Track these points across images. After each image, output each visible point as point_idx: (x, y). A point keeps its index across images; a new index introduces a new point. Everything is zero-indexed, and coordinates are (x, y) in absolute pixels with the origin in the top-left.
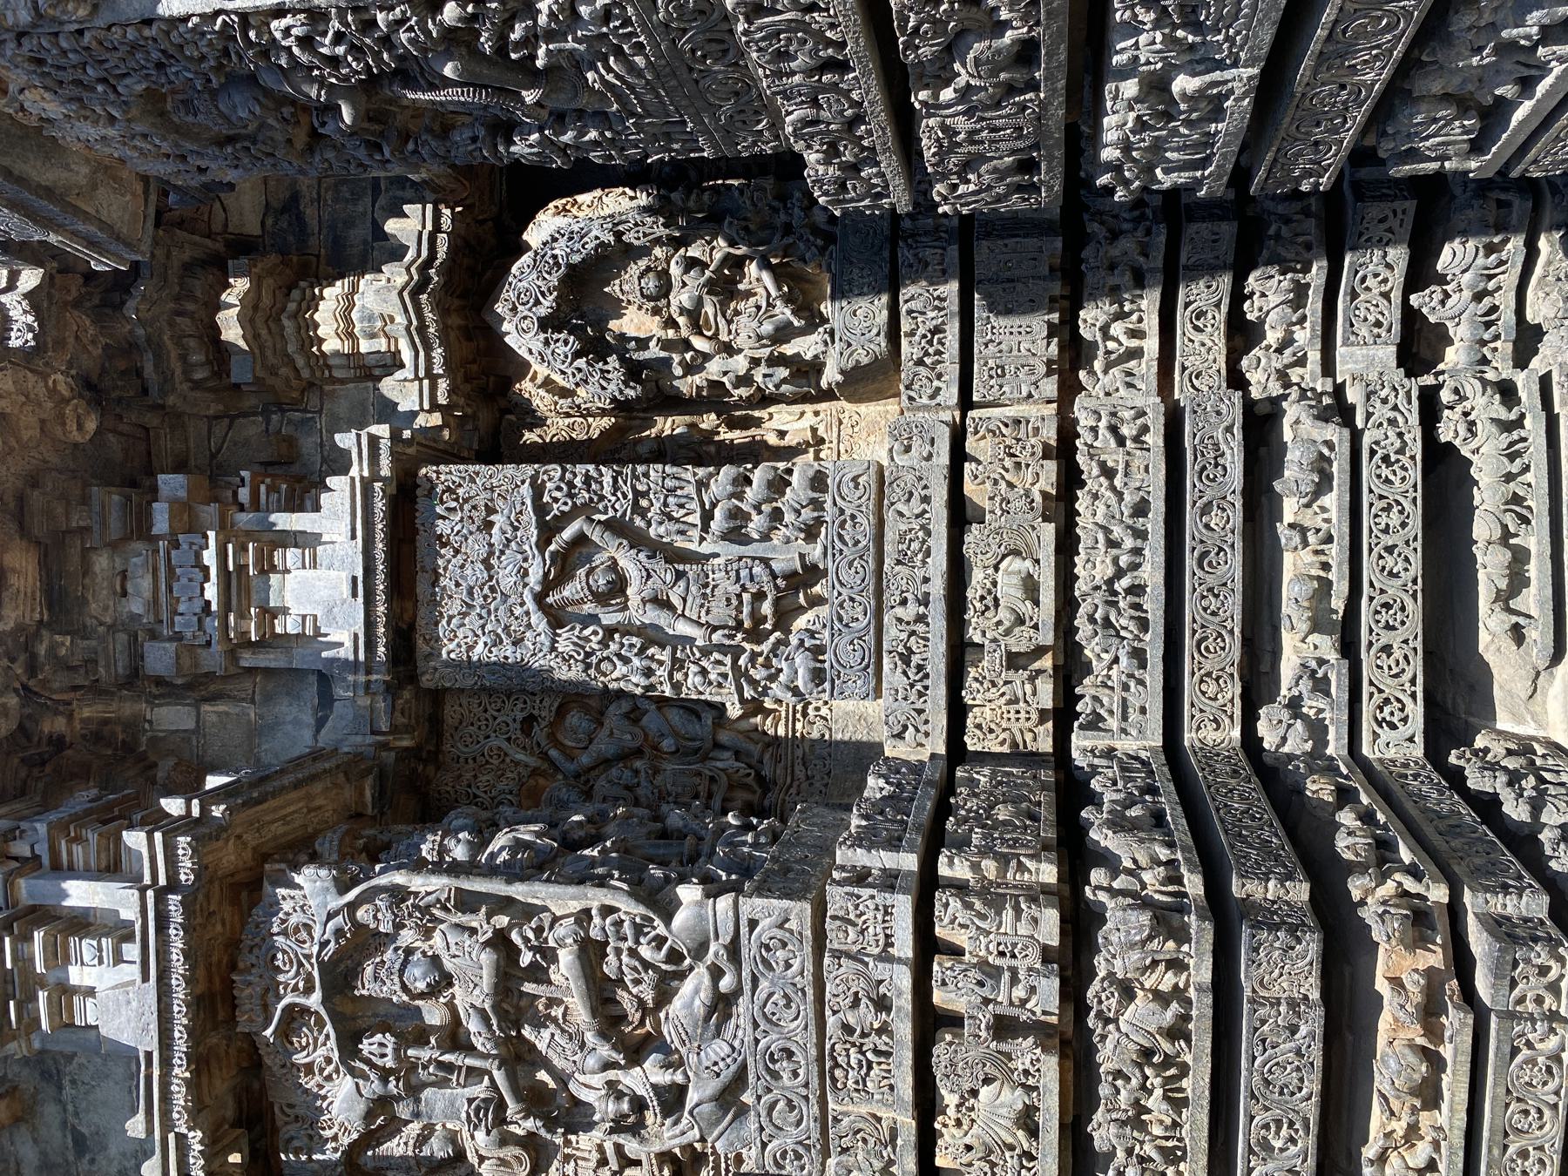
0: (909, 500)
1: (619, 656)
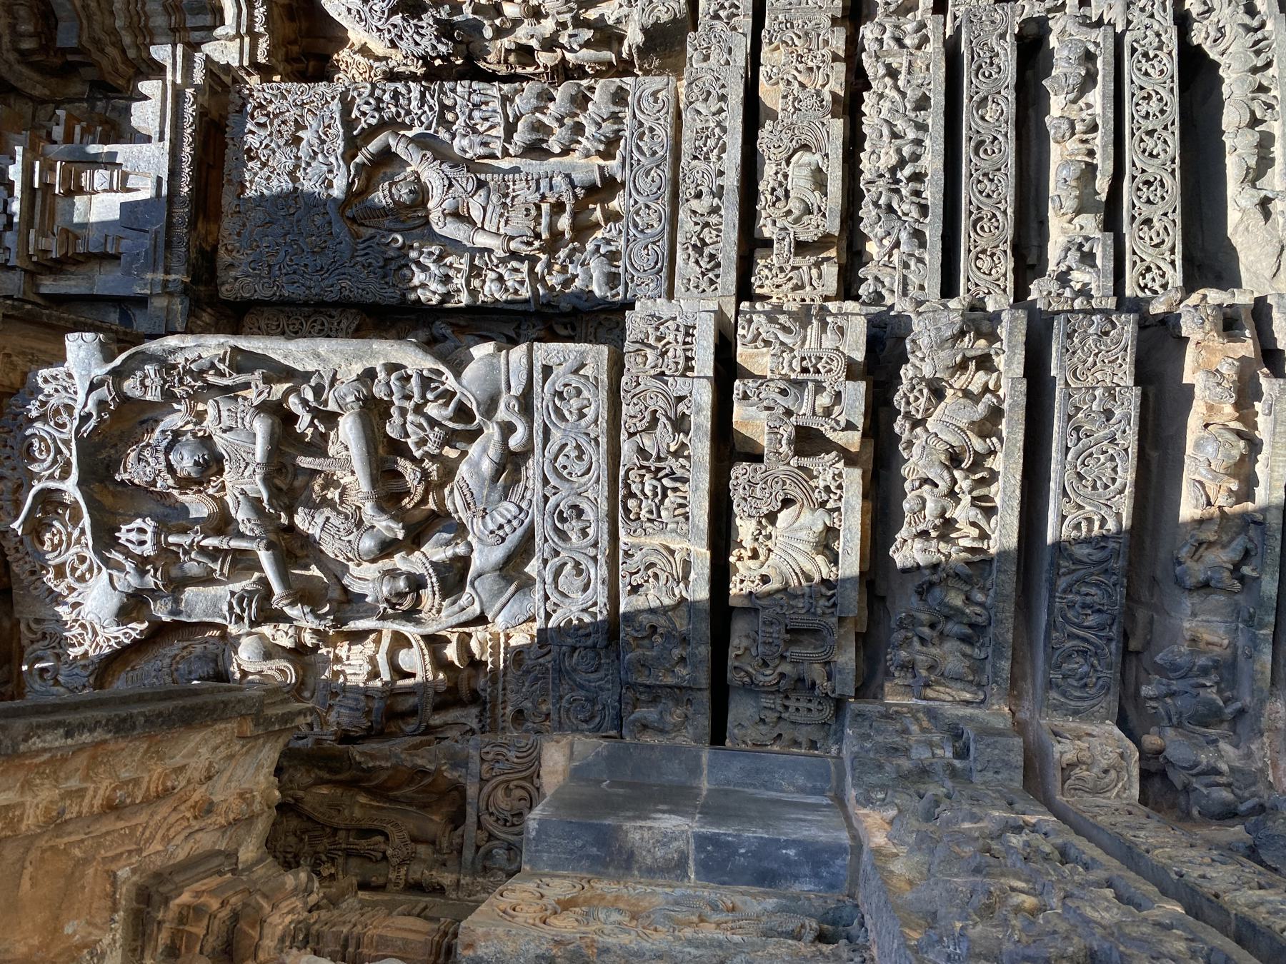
0: (706, 100)
1: (418, 263)
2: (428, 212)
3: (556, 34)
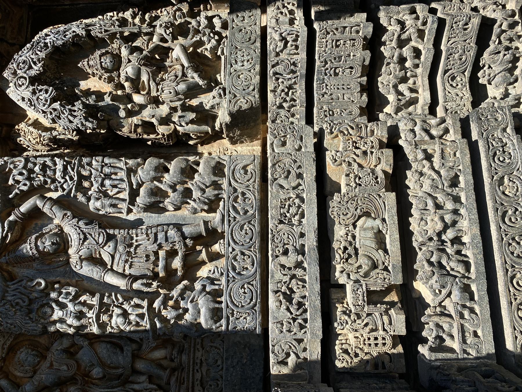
0: (287, 177)
2: (68, 257)
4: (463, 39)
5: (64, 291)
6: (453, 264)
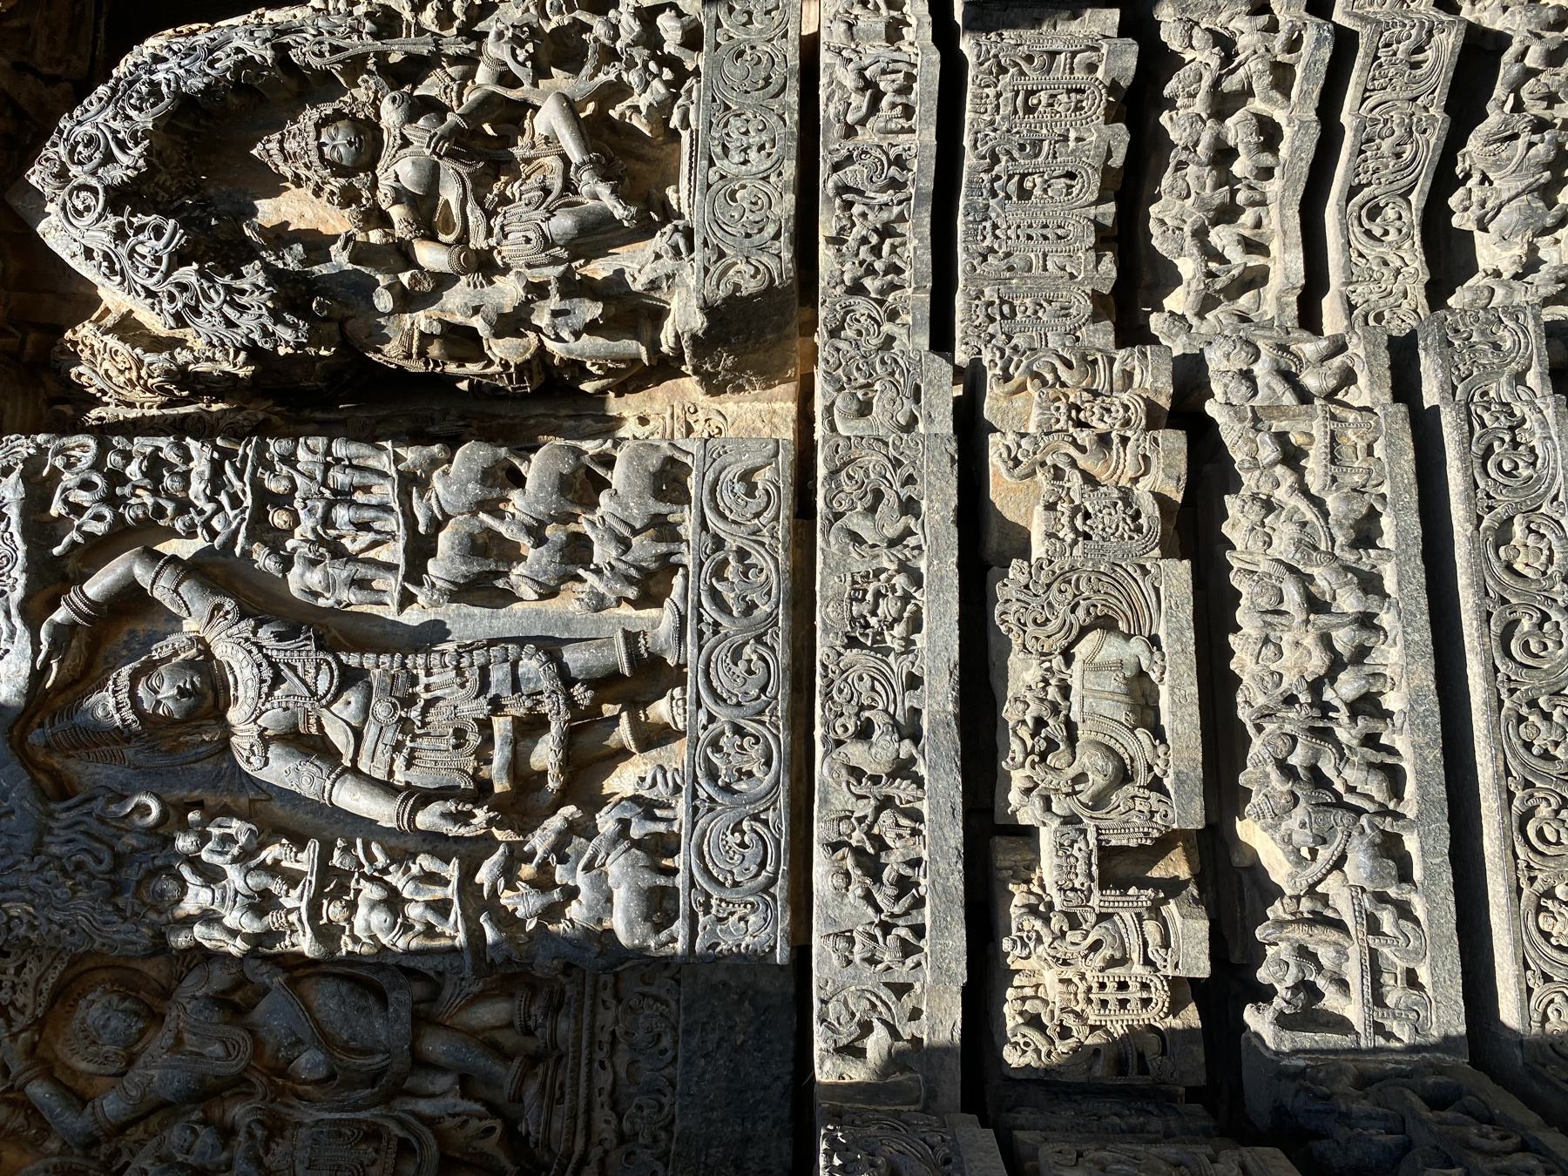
0: (872, 510)
1: (194, 862)
2: (228, 731)
3: (525, 309)
4: (1409, 95)
5: (215, 831)
6: (1352, 775)
